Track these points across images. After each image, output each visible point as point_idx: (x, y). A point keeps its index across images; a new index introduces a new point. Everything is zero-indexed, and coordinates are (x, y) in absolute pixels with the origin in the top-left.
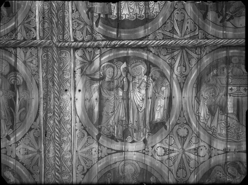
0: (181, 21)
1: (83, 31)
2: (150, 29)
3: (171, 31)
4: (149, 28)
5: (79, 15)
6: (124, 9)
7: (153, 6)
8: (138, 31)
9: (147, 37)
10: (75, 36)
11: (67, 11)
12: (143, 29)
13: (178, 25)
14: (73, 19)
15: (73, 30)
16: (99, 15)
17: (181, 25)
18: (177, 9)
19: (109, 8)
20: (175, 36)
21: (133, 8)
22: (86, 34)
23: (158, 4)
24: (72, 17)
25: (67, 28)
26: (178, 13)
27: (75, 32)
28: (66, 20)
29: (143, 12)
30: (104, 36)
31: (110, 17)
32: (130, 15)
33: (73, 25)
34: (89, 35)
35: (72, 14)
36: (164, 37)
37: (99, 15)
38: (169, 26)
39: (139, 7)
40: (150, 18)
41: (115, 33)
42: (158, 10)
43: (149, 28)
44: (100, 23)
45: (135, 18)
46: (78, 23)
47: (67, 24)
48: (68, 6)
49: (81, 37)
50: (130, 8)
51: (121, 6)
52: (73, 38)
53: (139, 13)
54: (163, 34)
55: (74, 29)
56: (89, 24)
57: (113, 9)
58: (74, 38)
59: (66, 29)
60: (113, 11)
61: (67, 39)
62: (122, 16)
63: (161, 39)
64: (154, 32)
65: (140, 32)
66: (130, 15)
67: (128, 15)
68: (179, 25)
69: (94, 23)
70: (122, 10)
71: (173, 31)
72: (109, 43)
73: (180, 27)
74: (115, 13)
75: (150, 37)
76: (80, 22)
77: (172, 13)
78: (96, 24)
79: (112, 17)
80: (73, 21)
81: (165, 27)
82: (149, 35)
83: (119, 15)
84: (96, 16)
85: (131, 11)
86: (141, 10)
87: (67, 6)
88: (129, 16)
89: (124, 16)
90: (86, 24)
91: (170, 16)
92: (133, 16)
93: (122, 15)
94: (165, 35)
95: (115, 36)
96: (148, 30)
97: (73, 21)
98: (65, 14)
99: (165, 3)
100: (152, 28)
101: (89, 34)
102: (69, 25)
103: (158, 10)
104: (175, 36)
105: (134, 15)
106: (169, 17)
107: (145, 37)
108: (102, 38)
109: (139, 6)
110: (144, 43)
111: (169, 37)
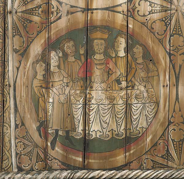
0: (179, 142)
1: (32, 156)
2: (133, 153)
3: (164, 155)
4: (132, 152)
5: (26, 132)
6: (94, 121)
7: (137, 118)
8: (115, 156)
9: (128, 165)
10: (20, 163)
11: (7, 126)
12: (123, 152)
13: (174, 147)
14: (16, 138)
15: (17, 154)
16: (57, 131)
17: (179, 147)
18: (174, 124)
19: (71, 121)
20: (170, 163)
21: (108, 121)
22: (37, 160)
23: (146, 115)
24: (15, 135)
25: (8, 151)
26: (175, 130)
27: (19, 158)
28: (7, 139)
29: (123, 127)
30: (63, 163)
31: (72, 135)
32: (103, 132)
33: (16, 146)
34: (41, 161)
35: (15, 129)
36: (153, 166)
37: (57, 131)
38: (161, 149)
39: (116, 120)
40: (132, 137)
41: (80, 159)
42: (145, 125)
43: (132, 152)
44: (58, 144)
45: (111, 136)
46: (24, 144)
47: (8, 144)
48: (10, 119)
49: (29, 165)
50: (103, 121)
51: (89, 118)
52: (16, 166)
53: (116, 130)
54: (152, 160)
55: (18, 154)
56: (40, 144)
57: (77, 124)
58: (17, 166)
59: (7, 152)
60: (77, 127)
61: (7, 168)
62: (90, 133)
63: (149, 167)
64: (139, 158)
65: (118, 158)
66: (103, 132)
67: (101, 132)
68: (176, 147)
69: (49, 144)
70: (91, 125)
71: (167, 156)
72: (71, 177)
73: (178, 150)
74: (80, 128)
75: (133, 165)
76: (27, 142)
77: (166, 129)
78: (51, 144)
79: (76, 135)
80: (17, 141)
81: (156, 149)
82: (132, 162)
83: (87, 132)
84: (52, 133)
85: (105, 126)
86: (119, 125)
87: (8, 118)
88: (101, 134)
89: (94, 134)
90: (37, 146)
91: (163, 134)
92: (107, 133)
93: (91, 132)
94: (155, 162)
95: (79, 164)
96: (130, 155)
97: (17, 141)
98: (5, 131)
99: (155, 115)
100: (136, 151)
101: (41, 160)
102: (11, 147)
103: (145, 125)
104: (170, 163)
105: (109, 131)
106: (161, 136)
107: (126, 165)
108: (60, 166)
109: (116, 118)
110: (124, 177)
111: (162, 165)
